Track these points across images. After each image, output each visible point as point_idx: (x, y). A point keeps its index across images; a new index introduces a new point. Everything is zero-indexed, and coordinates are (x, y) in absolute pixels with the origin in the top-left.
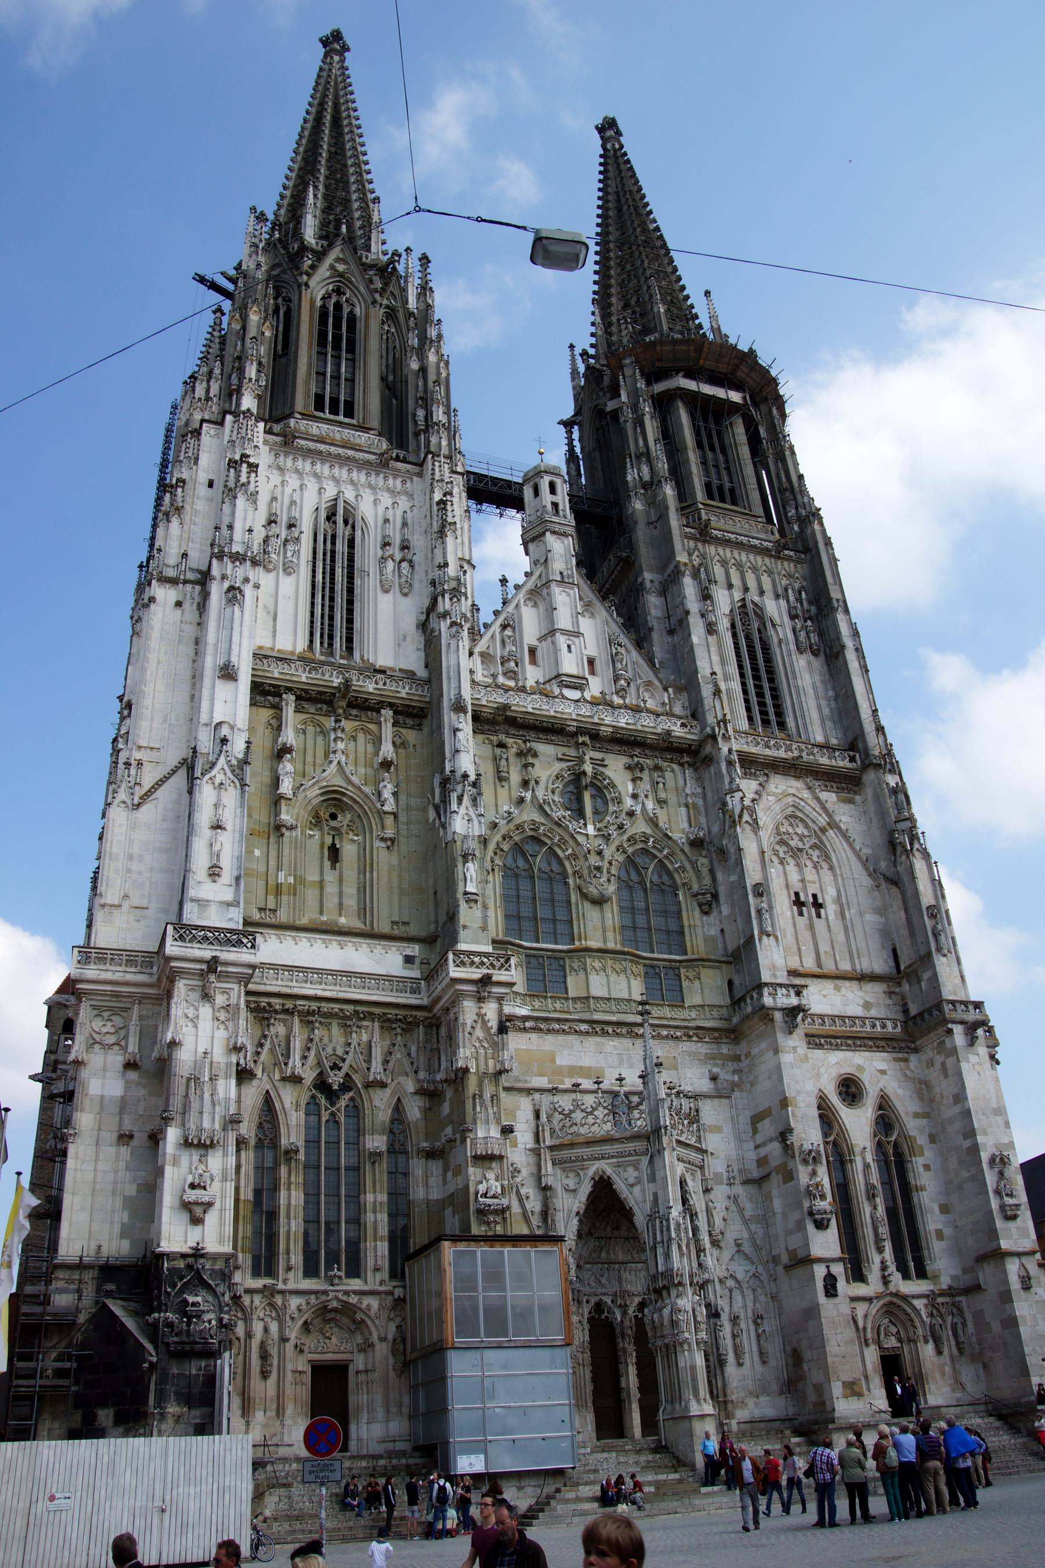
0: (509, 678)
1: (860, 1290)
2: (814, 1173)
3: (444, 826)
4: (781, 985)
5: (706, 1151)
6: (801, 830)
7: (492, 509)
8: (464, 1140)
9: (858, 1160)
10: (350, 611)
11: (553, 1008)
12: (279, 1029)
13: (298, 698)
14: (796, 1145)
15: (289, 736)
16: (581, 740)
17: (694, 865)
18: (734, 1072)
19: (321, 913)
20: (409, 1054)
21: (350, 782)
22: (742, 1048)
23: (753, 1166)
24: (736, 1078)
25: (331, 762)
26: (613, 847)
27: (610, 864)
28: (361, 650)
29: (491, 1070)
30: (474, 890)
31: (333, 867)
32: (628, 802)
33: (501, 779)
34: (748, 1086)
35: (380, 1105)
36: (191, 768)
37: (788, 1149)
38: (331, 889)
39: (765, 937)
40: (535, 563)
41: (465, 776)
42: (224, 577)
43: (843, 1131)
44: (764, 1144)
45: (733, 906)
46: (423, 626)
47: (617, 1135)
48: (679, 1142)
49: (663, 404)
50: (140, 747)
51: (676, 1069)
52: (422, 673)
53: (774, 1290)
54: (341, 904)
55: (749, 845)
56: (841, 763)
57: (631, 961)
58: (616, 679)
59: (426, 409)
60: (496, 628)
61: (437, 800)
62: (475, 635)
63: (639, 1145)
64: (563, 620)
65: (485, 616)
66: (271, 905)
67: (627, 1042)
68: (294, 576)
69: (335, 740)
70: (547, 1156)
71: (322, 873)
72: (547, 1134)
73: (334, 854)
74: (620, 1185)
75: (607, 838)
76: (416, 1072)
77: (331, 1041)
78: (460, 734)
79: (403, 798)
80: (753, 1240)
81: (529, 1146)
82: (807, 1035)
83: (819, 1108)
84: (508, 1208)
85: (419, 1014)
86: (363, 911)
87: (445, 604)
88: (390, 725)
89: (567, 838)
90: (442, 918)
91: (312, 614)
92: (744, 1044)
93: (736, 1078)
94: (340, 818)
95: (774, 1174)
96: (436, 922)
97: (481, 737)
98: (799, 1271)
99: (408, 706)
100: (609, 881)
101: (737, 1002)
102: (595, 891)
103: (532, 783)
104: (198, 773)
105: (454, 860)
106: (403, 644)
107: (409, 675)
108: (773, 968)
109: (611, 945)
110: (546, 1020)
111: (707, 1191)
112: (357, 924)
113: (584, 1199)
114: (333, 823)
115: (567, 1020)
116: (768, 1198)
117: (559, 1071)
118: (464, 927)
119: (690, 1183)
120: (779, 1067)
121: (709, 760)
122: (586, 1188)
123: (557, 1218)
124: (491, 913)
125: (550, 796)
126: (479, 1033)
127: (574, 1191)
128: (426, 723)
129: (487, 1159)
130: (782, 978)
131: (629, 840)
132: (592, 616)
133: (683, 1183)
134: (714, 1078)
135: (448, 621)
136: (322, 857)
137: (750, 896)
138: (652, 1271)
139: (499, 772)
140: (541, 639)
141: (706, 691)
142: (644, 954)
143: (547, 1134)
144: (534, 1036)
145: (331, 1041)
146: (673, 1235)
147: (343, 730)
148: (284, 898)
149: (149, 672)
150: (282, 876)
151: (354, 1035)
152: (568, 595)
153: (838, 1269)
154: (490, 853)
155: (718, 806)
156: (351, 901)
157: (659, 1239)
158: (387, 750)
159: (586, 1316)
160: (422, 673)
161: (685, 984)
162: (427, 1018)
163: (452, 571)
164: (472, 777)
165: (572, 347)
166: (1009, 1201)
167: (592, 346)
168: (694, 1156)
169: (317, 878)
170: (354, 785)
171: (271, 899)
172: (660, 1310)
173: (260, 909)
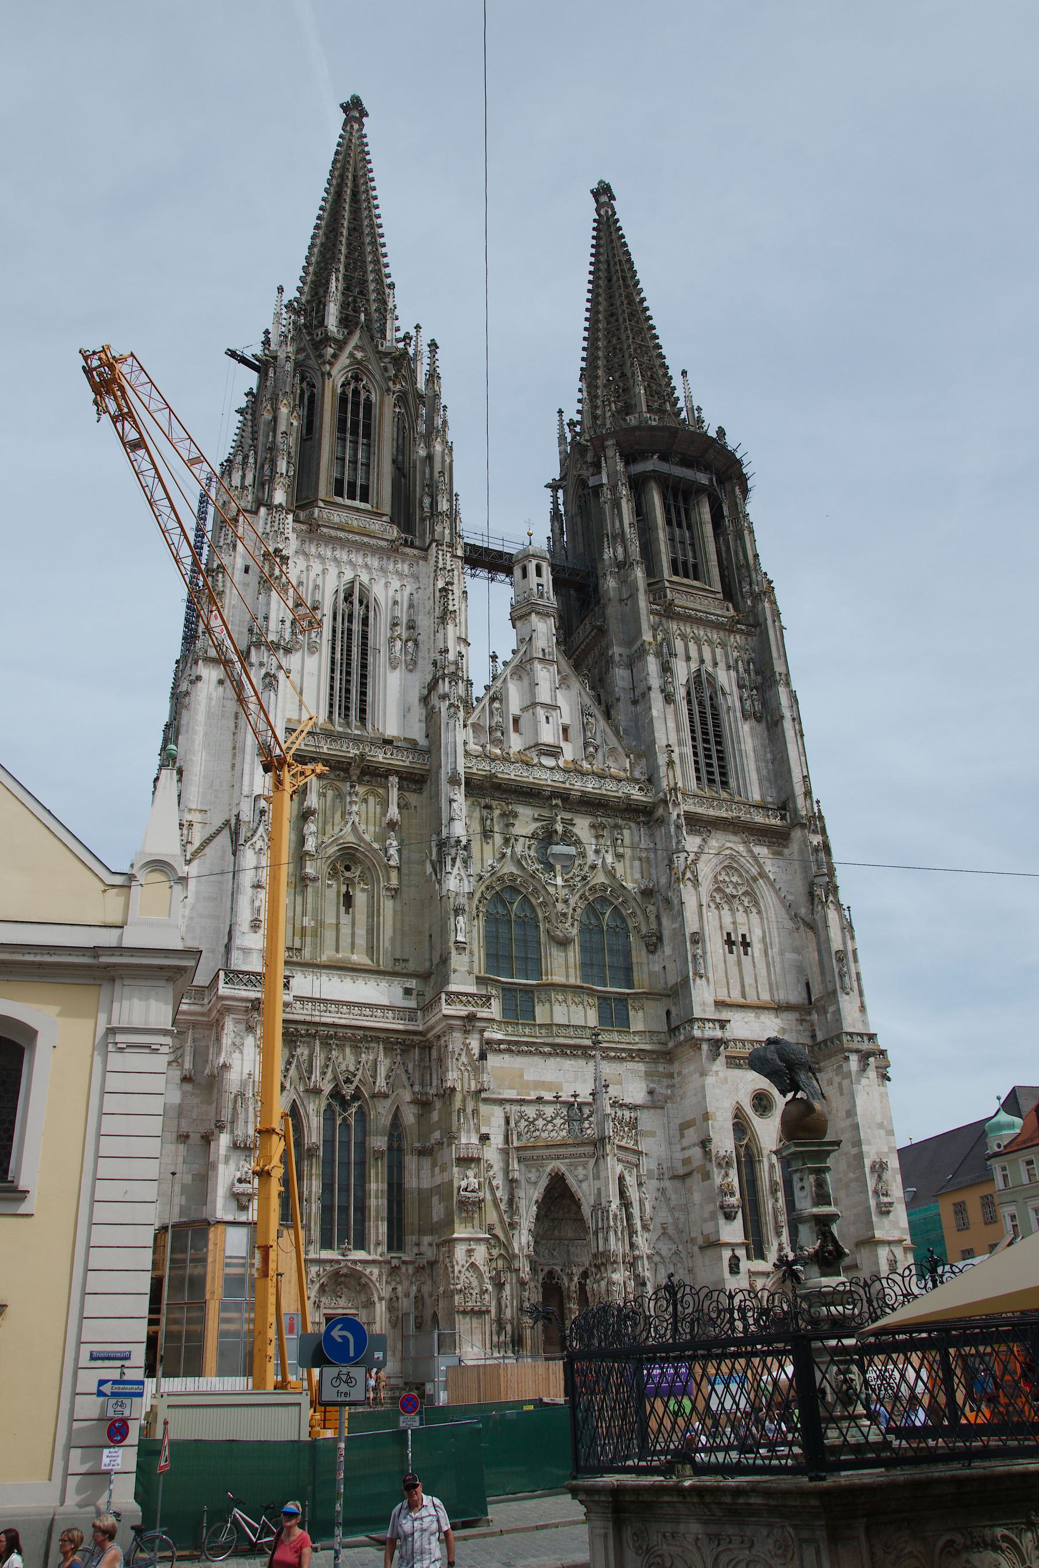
0: (496, 746)
1: (759, 1265)
2: (727, 1175)
3: (439, 882)
4: (709, 1020)
5: (642, 1152)
7: (483, 573)
8: (450, 1144)
9: (765, 1160)
10: (363, 685)
11: (523, 1034)
12: (302, 1051)
14: (714, 1152)
15: (313, 800)
16: (554, 802)
17: (644, 911)
18: (668, 1087)
19: (337, 951)
20: (407, 1071)
21: (361, 839)
22: (676, 1067)
23: (679, 1164)
25: (347, 822)
26: (577, 896)
27: (574, 910)
28: (373, 720)
29: (473, 1088)
30: (463, 940)
31: (347, 912)
34: (678, 1099)
35: (381, 1114)
36: (235, 835)
37: (707, 1153)
38: (345, 931)
39: (698, 979)
40: (521, 641)
41: (458, 842)
42: (262, 664)
43: (754, 1137)
44: (689, 1147)
45: (674, 949)
46: (425, 700)
47: (570, 1141)
48: (620, 1147)
49: (638, 485)
50: (190, 810)
52: (422, 742)
53: (691, 1265)
54: (353, 944)
55: (689, 896)
58: (586, 744)
59: (432, 497)
60: (486, 701)
61: (434, 857)
62: (469, 707)
63: (589, 1149)
64: (544, 694)
65: (478, 691)
66: (297, 945)
67: (582, 1062)
68: (317, 654)
70: (514, 1155)
71: (338, 917)
72: (515, 1137)
73: (348, 901)
74: (571, 1181)
75: (572, 888)
76: (412, 1086)
77: (344, 1059)
78: (454, 805)
79: (405, 852)
80: (676, 1224)
81: (500, 1146)
83: (736, 1116)
84: (483, 1200)
85: (415, 1038)
86: (371, 950)
87: (444, 687)
88: (395, 790)
89: (540, 888)
90: (436, 960)
91: (332, 688)
92: (676, 1064)
93: (669, 1092)
95: (695, 1173)
96: (431, 960)
97: (472, 799)
98: (710, 1252)
99: (411, 773)
100: (573, 925)
101: (673, 1031)
102: (561, 934)
103: (513, 840)
104: (241, 841)
105: (448, 913)
106: (408, 715)
107: (412, 746)
108: (704, 1004)
109: (572, 981)
110: (516, 1043)
111: (640, 1185)
113: (542, 1190)
114: (347, 874)
116: (690, 1191)
117: (526, 1086)
118: (455, 971)
119: (627, 1178)
120: (703, 1087)
121: (662, 821)
122: (544, 1182)
123: (520, 1205)
124: (476, 958)
126: (464, 1059)
127: (535, 1183)
128: (427, 786)
129: (466, 1162)
130: (711, 1013)
131: (590, 889)
133: (621, 1179)
134: (651, 1092)
135: (447, 703)
136: (338, 904)
137: (688, 943)
138: (594, 1250)
140: (523, 710)
141: (662, 759)
142: (599, 988)
143: (515, 1137)
144: (506, 1056)
145: (344, 1059)
146: (612, 1224)
148: (308, 939)
149: (197, 743)
150: (306, 920)
151: (363, 1055)
152: (549, 671)
153: (741, 1253)
154: (476, 901)
155: (666, 862)
156: (361, 941)
157: (600, 1226)
158: (393, 812)
159: (540, 1281)
160: (422, 742)
161: (631, 1013)
162: (421, 1041)
163: (451, 656)
164: (464, 842)
165: (560, 412)
166: (885, 1199)
167: (579, 412)
168: (632, 1158)
169: (334, 921)
170: (365, 842)
171: (297, 940)
172: (598, 1282)
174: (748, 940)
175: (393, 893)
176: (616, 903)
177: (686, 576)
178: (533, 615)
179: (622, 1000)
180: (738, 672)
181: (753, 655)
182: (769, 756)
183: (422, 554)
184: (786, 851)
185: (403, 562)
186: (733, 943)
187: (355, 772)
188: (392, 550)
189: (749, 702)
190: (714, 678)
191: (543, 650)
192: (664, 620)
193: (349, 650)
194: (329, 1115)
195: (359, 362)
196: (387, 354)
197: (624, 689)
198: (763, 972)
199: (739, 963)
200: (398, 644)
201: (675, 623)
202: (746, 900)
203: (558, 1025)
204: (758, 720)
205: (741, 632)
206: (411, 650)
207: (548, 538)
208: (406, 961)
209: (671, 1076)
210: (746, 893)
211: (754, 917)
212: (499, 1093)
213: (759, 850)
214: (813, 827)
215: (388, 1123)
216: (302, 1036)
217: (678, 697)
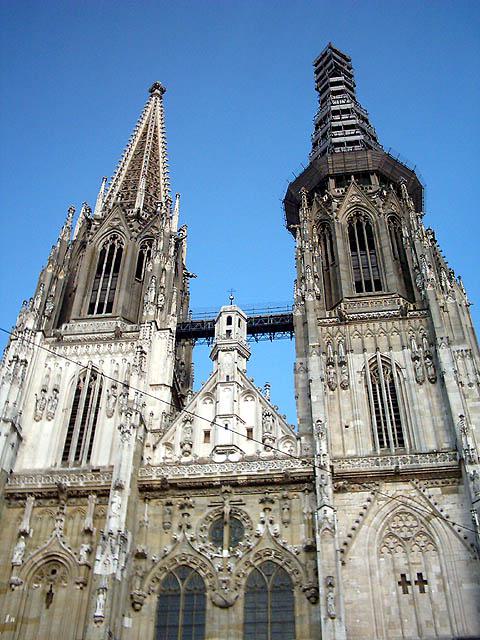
6: (411, 522)
13: (37, 498)
15: (25, 526)
16: (224, 488)
31: (48, 607)
32: (260, 529)
38: (43, 622)
39: (330, 620)
41: (111, 534)
56: (441, 463)
89: (207, 563)
103: (184, 527)
114: (53, 577)
174: (424, 579)
176: (280, 563)
177: (369, 289)
185: (127, 343)
186: (409, 583)
188: (118, 335)
189: (421, 369)
198: (442, 607)
199: (413, 602)
201: (353, 327)
202: (422, 540)
204: (433, 381)
213: (431, 491)
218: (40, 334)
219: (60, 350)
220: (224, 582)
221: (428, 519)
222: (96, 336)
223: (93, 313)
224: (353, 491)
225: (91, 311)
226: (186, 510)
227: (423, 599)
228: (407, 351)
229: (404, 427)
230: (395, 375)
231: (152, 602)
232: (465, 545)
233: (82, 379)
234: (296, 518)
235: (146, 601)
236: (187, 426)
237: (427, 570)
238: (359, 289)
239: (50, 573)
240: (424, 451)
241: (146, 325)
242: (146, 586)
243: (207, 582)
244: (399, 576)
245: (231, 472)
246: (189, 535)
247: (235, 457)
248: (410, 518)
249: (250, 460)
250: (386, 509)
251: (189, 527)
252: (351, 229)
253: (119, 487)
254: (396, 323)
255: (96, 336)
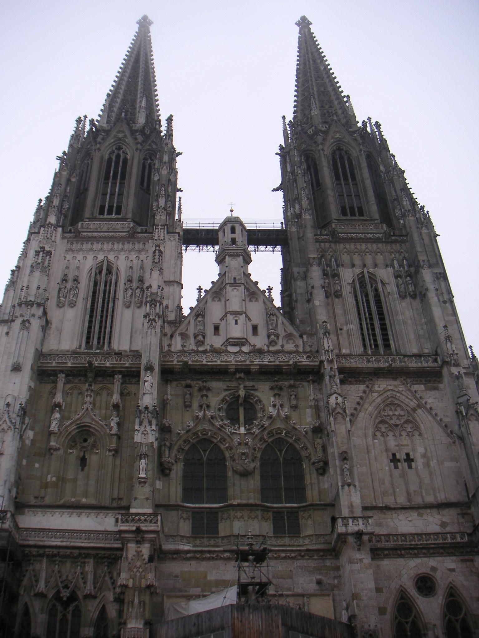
13: (67, 375)
14: (359, 626)
15: (59, 398)
16: (238, 376)
18: (335, 577)
21: (93, 419)
24: (336, 581)
26: (257, 439)
30: (144, 476)
31: (82, 470)
32: (271, 409)
33: (186, 406)
38: (80, 483)
39: (346, 487)
51: (292, 578)
56: (425, 365)
57: (262, 510)
69: (87, 396)
73: (83, 462)
76: (114, 588)
82: (372, 550)
89: (226, 437)
93: (336, 581)
94: (89, 441)
102: (241, 468)
103: (204, 406)
109: (252, 501)
110: (201, 552)
112: (92, 501)
114: (85, 444)
115: (215, 551)
118: (136, 498)
125: (217, 412)
131: (268, 434)
132: (257, 300)
134: (319, 583)
135: (148, 319)
139: (185, 402)
144: (194, 563)
147: (92, 391)
148: (49, 490)
156: (91, 489)
158: (116, 398)
161: (302, 522)
173: (36, 497)
174: (412, 457)
175: (113, 452)
176: (291, 441)
177: (353, 214)
178: (227, 257)
179: (294, 514)
180: (394, 268)
181: (407, 255)
182: (423, 320)
183: (150, 235)
184: (441, 386)
185: (139, 242)
186: (399, 461)
187: (90, 375)
188: (132, 236)
189: (403, 286)
190: (375, 276)
191: (235, 278)
192: (333, 245)
193: (103, 305)
194: (52, 613)
195: (120, 139)
196: (136, 131)
197: (301, 294)
198: (427, 480)
200: (130, 292)
201: (342, 246)
202: (409, 427)
203: (237, 536)
204: (414, 297)
205: (395, 242)
206: (138, 295)
207: (282, 223)
208: (120, 499)
209: (337, 568)
210: (407, 422)
211: (417, 437)
212: (186, 591)
213: (416, 387)
214: (453, 362)
215: (95, 616)
216: (34, 556)
217: (344, 293)
218: (60, 230)
219: (76, 246)
220: (243, 454)
221: (414, 410)
222: (111, 234)
223: (103, 214)
224: (351, 383)
225: (102, 212)
226: (205, 392)
227: (411, 474)
228: (390, 270)
229: (390, 333)
230: (380, 289)
231: (178, 470)
232: (446, 432)
233: (98, 272)
234: (302, 404)
235: (174, 467)
236: (199, 319)
237: (414, 449)
238: (344, 213)
239: (82, 440)
240: (408, 354)
241: (160, 227)
242: (173, 455)
243: (227, 454)
244: (390, 454)
245: (245, 361)
246: (208, 414)
247: (245, 349)
248: (398, 409)
249: (260, 352)
250: (379, 400)
251: (208, 406)
252: (334, 159)
253: (149, 368)
254: (380, 245)
255: (111, 234)
